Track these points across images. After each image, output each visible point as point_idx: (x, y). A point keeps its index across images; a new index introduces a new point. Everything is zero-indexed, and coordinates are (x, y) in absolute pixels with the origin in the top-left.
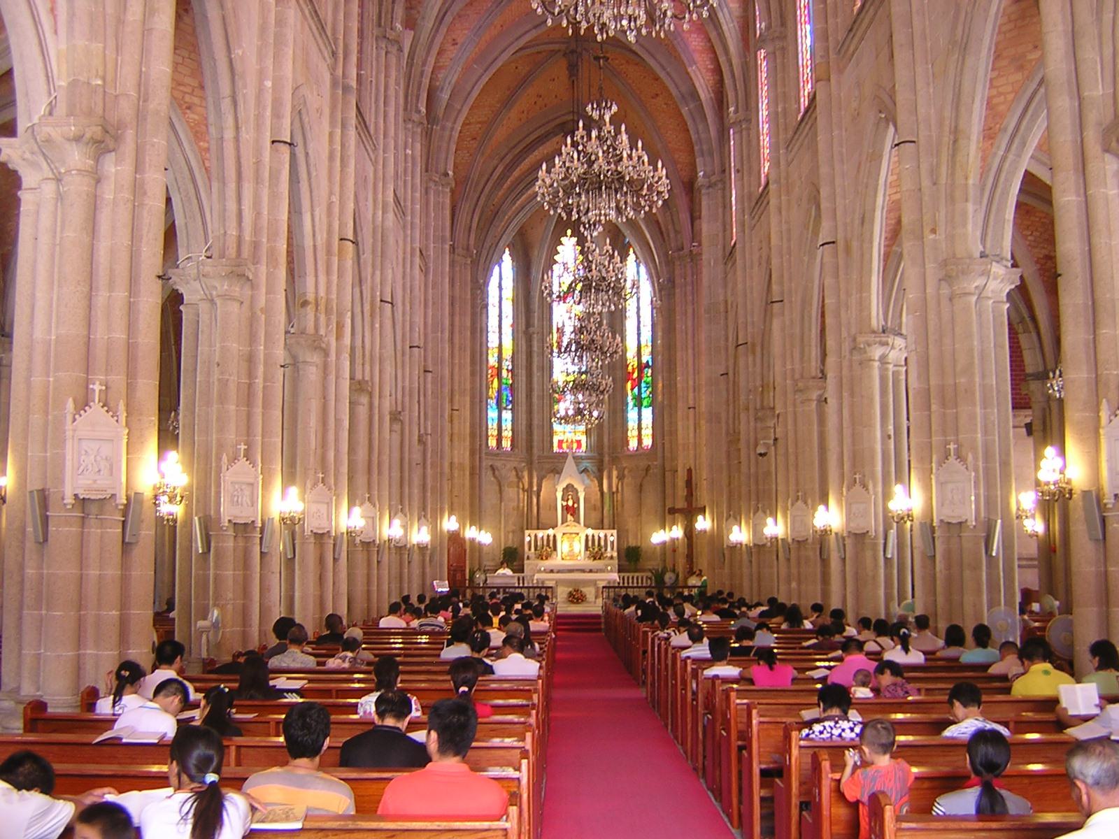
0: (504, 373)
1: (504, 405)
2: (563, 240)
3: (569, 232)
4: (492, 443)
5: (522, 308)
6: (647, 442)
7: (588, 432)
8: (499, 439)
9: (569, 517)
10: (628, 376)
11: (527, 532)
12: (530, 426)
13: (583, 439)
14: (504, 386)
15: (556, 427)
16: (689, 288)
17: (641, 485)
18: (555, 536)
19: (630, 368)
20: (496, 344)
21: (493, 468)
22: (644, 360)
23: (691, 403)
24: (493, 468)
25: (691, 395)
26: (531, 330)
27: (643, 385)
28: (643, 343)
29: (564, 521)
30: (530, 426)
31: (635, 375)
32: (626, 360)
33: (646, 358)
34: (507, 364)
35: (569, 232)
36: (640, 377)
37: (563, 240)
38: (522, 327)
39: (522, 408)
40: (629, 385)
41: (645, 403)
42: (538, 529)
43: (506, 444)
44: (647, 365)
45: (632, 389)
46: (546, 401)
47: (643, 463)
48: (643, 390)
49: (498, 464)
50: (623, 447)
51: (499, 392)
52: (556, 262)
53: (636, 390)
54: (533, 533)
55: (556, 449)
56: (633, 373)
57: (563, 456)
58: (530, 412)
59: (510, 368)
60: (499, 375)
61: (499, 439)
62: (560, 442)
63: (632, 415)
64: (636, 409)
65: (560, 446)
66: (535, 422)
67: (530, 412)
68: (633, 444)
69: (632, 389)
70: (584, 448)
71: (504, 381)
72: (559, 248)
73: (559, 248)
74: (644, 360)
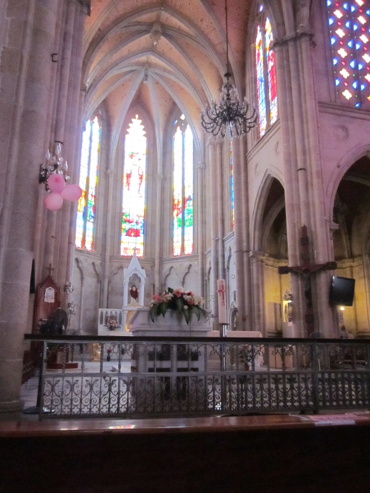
0: (90, 197)
1: (88, 218)
2: (133, 120)
3: (137, 116)
4: (78, 243)
5: (104, 156)
6: (189, 250)
7: (145, 244)
8: (84, 241)
9: (132, 299)
10: (173, 207)
11: (100, 310)
12: (105, 235)
13: (141, 248)
14: (89, 205)
15: (124, 238)
16: (292, 66)
17: (184, 279)
18: (120, 314)
19: (176, 202)
20: (86, 175)
21: (77, 260)
22: (187, 196)
23: (300, 165)
24: (77, 260)
25: (299, 158)
26: (109, 171)
27: (186, 212)
28: (186, 185)
29: (129, 302)
30: (105, 235)
31: (180, 206)
32: (173, 196)
33: (189, 192)
34: (92, 191)
35: (137, 116)
36: (184, 207)
37: (133, 120)
38: (104, 168)
39: (100, 222)
40: (175, 212)
41: (187, 223)
42: (108, 308)
43: (88, 246)
44: (189, 199)
45: (177, 215)
46: (117, 220)
47: (186, 264)
48: (186, 215)
49: (81, 258)
50: (169, 253)
51: (86, 208)
52: (127, 133)
53: (180, 216)
54: (104, 310)
55: (122, 253)
56: (178, 205)
57: (128, 259)
58: (105, 226)
59: (94, 194)
60: (86, 197)
61: (84, 241)
62: (126, 249)
63: (177, 232)
64: (180, 229)
65: (126, 252)
66: (109, 233)
67: (105, 226)
68: (177, 252)
69: (177, 215)
70: (141, 254)
71: (89, 202)
72: (130, 125)
73: (130, 125)
74: (187, 196)
